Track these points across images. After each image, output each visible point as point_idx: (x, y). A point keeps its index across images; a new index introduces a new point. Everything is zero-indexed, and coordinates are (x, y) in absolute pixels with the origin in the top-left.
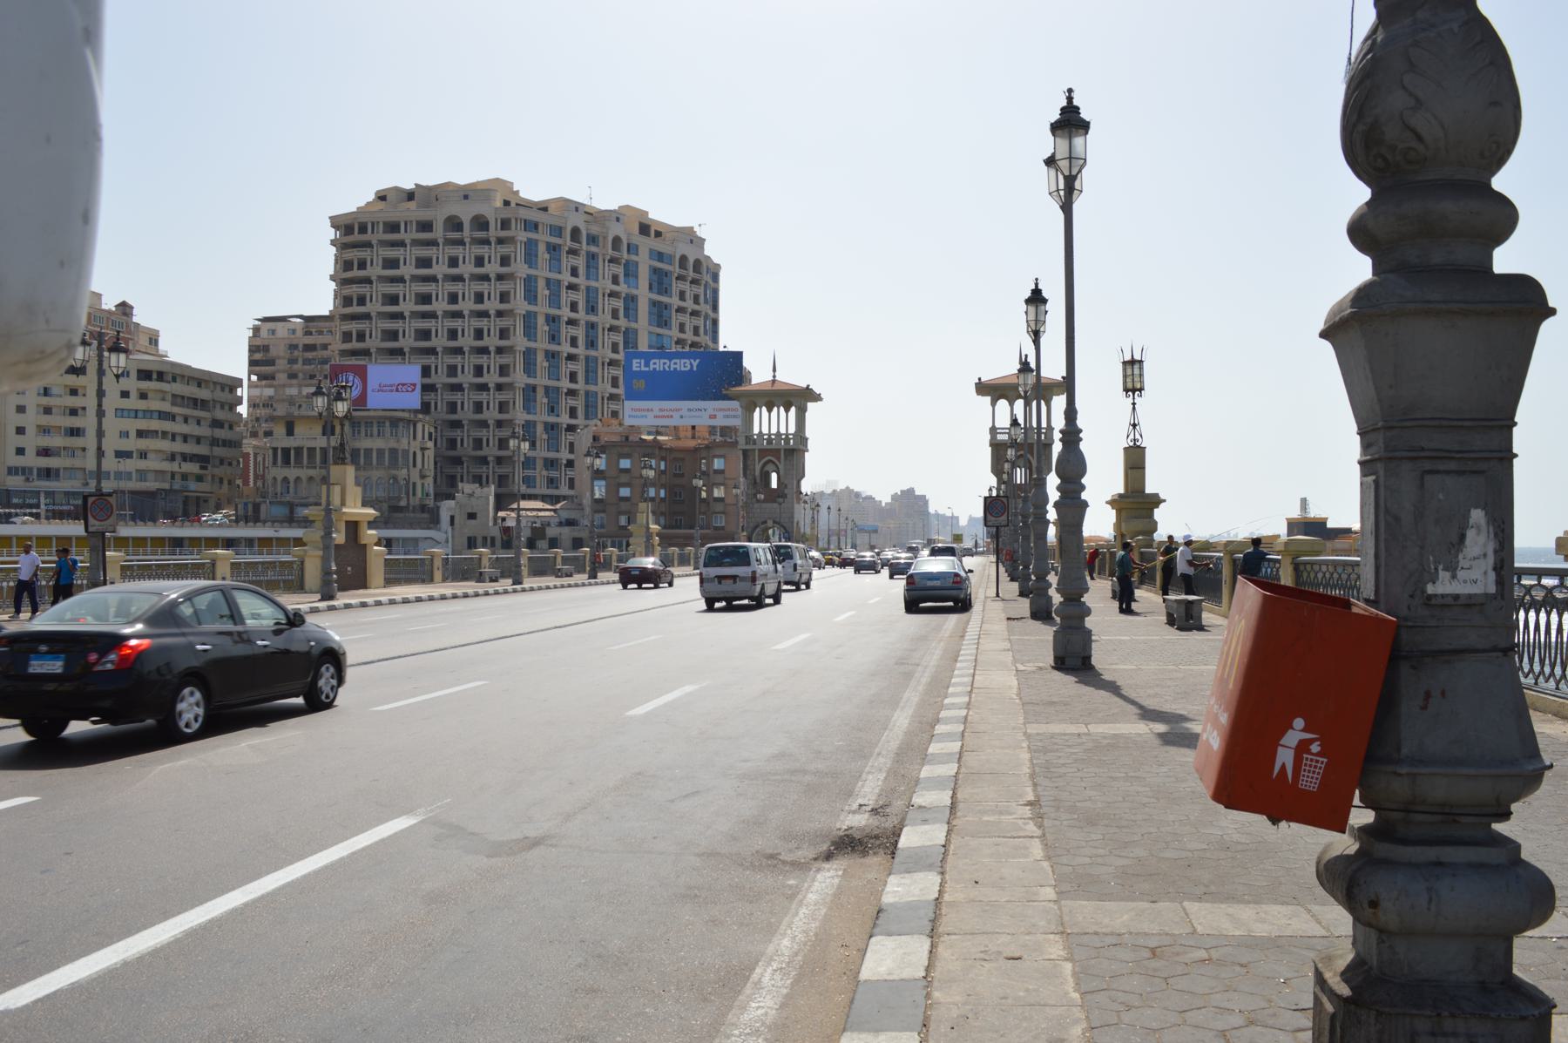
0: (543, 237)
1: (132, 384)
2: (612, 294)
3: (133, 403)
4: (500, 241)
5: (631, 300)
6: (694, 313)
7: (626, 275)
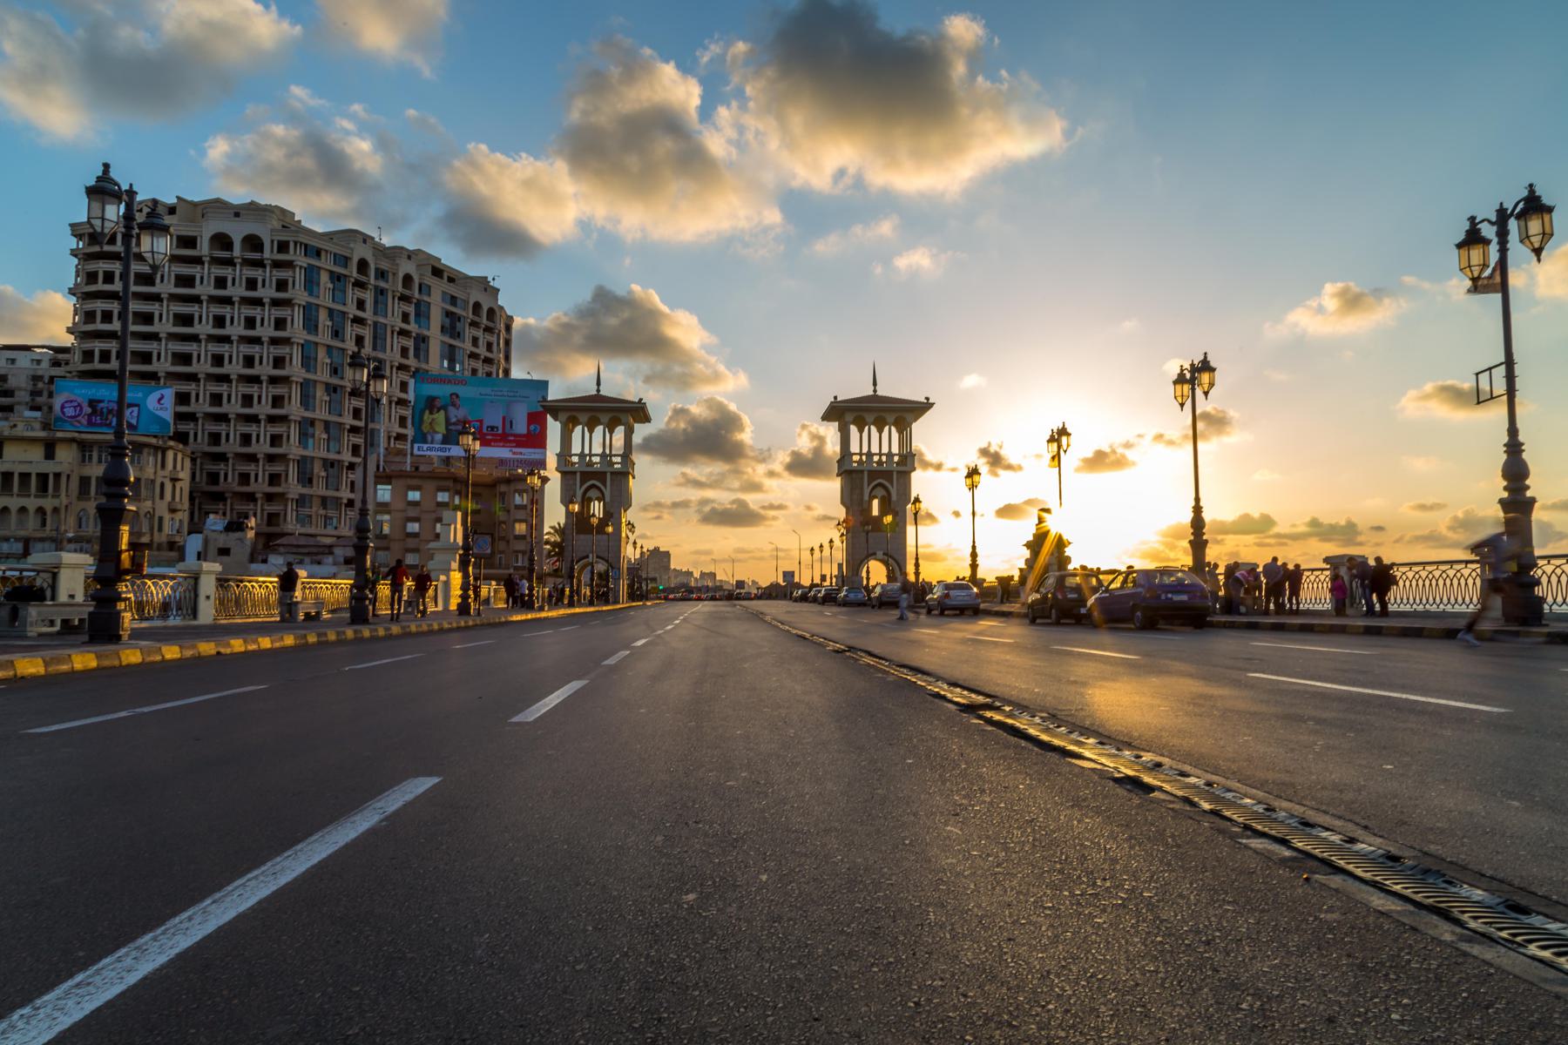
2: (402, 333)
5: (422, 340)
6: (488, 361)
7: (418, 315)
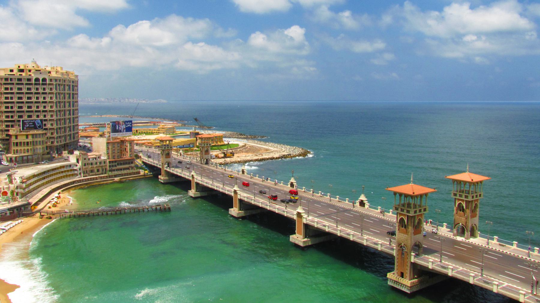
4: (49, 84)
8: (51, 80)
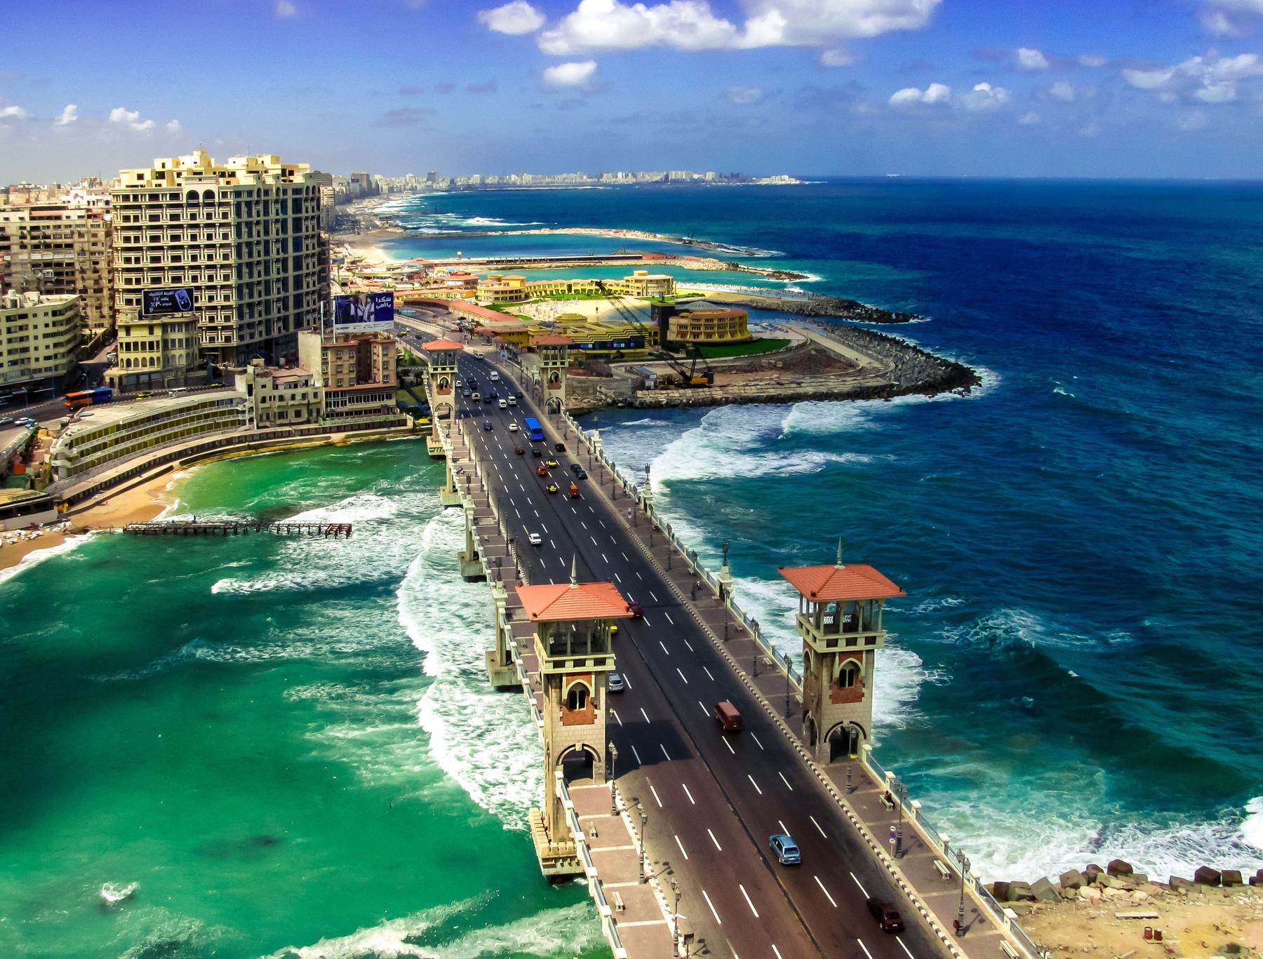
0: (245, 198)
1: (50, 319)
3: (51, 330)
4: (221, 204)
8: (225, 195)
